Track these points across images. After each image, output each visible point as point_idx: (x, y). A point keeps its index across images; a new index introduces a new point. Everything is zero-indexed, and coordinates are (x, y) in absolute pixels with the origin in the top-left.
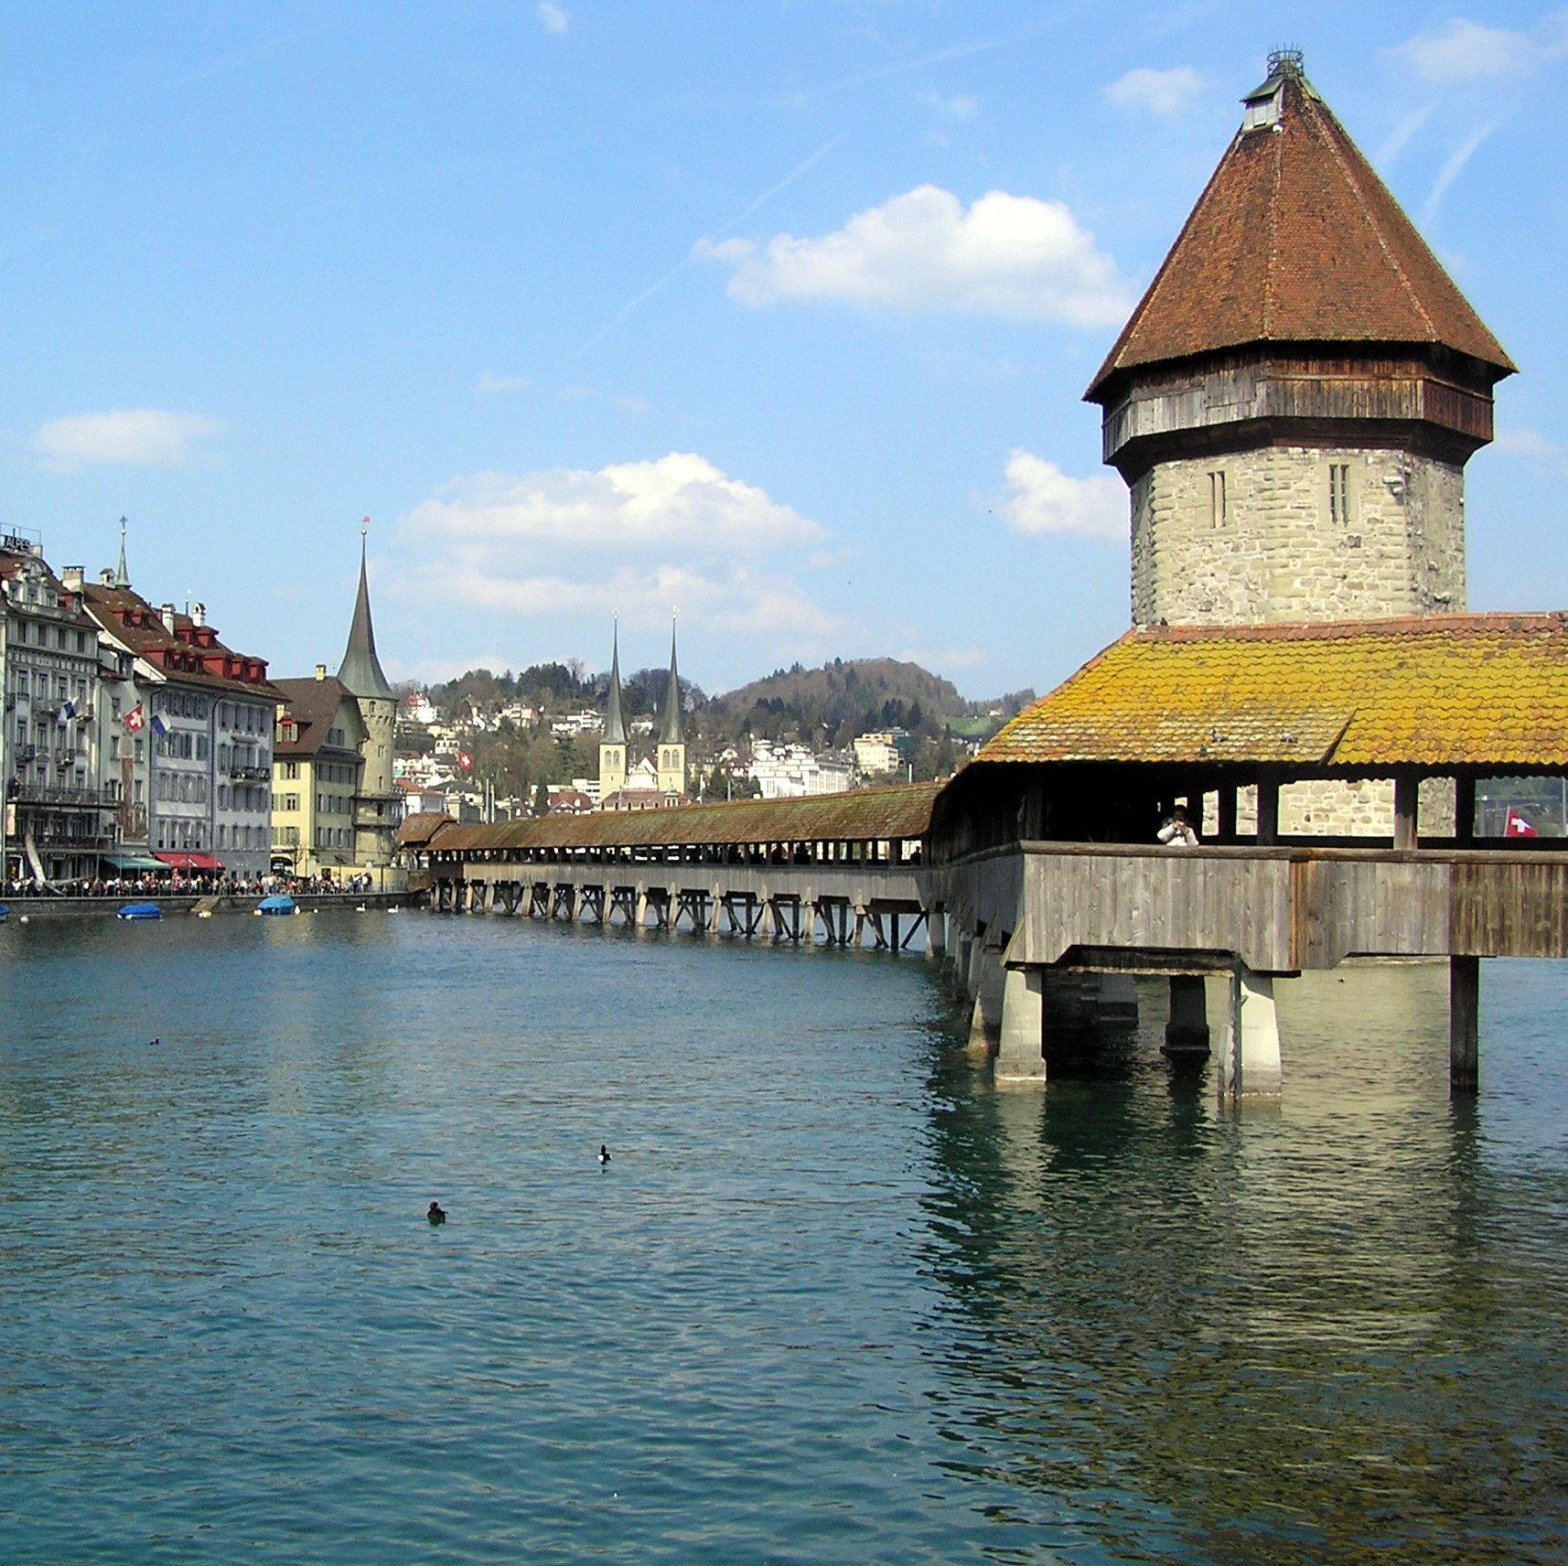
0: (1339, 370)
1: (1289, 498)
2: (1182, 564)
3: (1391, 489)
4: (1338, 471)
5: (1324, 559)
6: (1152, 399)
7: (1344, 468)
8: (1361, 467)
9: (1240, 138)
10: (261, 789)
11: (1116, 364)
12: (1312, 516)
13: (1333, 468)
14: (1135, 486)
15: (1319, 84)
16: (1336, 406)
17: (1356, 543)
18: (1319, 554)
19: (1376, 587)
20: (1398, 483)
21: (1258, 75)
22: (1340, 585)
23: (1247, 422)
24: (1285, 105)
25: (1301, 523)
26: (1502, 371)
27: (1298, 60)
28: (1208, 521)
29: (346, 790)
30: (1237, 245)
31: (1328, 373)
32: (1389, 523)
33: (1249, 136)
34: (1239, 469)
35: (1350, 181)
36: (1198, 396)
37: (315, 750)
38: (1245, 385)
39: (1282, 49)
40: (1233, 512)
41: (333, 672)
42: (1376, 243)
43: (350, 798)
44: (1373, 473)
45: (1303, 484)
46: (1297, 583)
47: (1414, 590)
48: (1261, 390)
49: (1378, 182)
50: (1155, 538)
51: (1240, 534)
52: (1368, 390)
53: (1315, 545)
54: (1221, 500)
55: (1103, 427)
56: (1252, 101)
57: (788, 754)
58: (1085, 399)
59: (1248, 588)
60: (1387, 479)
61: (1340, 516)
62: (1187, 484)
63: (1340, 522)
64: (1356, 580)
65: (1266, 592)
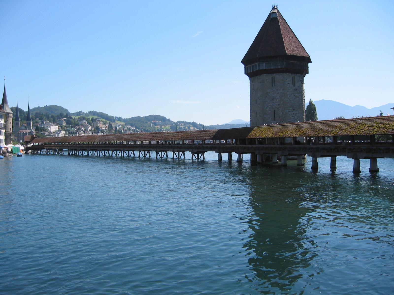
9: (270, 19)
11: (257, 57)
13: (293, 77)
14: (251, 78)
20: (302, 80)
33: (272, 19)
34: (278, 77)
39: (275, 4)
48: (285, 63)
53: (290, 90)
54: (273, 81)
55: (244, 67)
59: (280, 96)
60: (300, 79)
61: (294, 85)
63: (294, 86)
64: (296, 96)
65: (283, 98)
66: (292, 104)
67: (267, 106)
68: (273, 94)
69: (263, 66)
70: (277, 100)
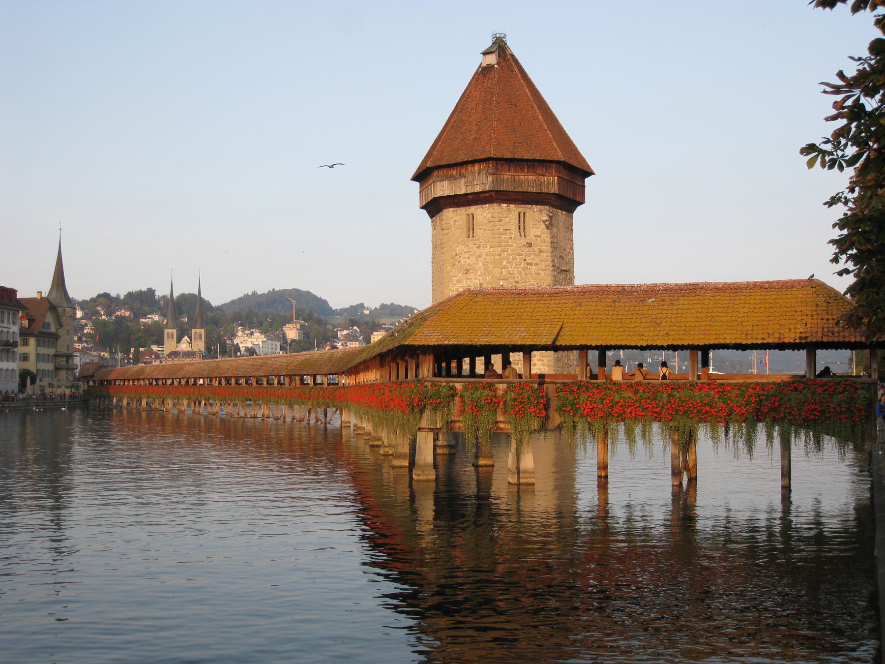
0: (522, 170)
1: (501, 225)
2: (455, 253)
3: (544, 223)
4: (522, 215)
5: (516, 252)
6: (443, 181)
7: (524, 214)
8: (532, 213)
9: (480, 69)
10: (14, 352)
11: (427, 166)
12: (511, 233)
13: (519, 214)
15: (515, 47)
16: (522, 186)
17: (530, 245)
18: (514, 250)
19: (538, 264)
20: (546, 220)
21: (488, 44)
22: (523, 263)
23: (484, 192)
24: (499, 56)
25: (507, 237)
26: (589, 173)
27: (504, 37)
28: (465, 235)
29: (51, 351)
30: (480, 115)
31: (518, 172)
32: (544, 236)
33: (484, 69)
34: (482, 213)
35: (527, 90)
36: (463, 181)
37: (37, 333)
38: (483, 175)
40: (478, 231)
41: (44, 295)
42: (538, 118)
43: (54, 355)
44: (537, 216)
45: (507, 220)
46: (505, 263)
47: (554, 266)
48: (490, 178)
49: (538, 91)
50: (443, 241)
51: (481, 241)
52: (535, 181)
55: (420, 192)
56: (485, 53)
57: (252, 333)
58: (412, 180)
59: (483, 264)
60: (543, 218)
61: (523, 234)
62: (457, 218)
64: (530, 262)
65: (492, 266)
66: (517, 282)
67: (453, 288)
68: (469, 258)
69: (442, 188)
70: (479, 273)
